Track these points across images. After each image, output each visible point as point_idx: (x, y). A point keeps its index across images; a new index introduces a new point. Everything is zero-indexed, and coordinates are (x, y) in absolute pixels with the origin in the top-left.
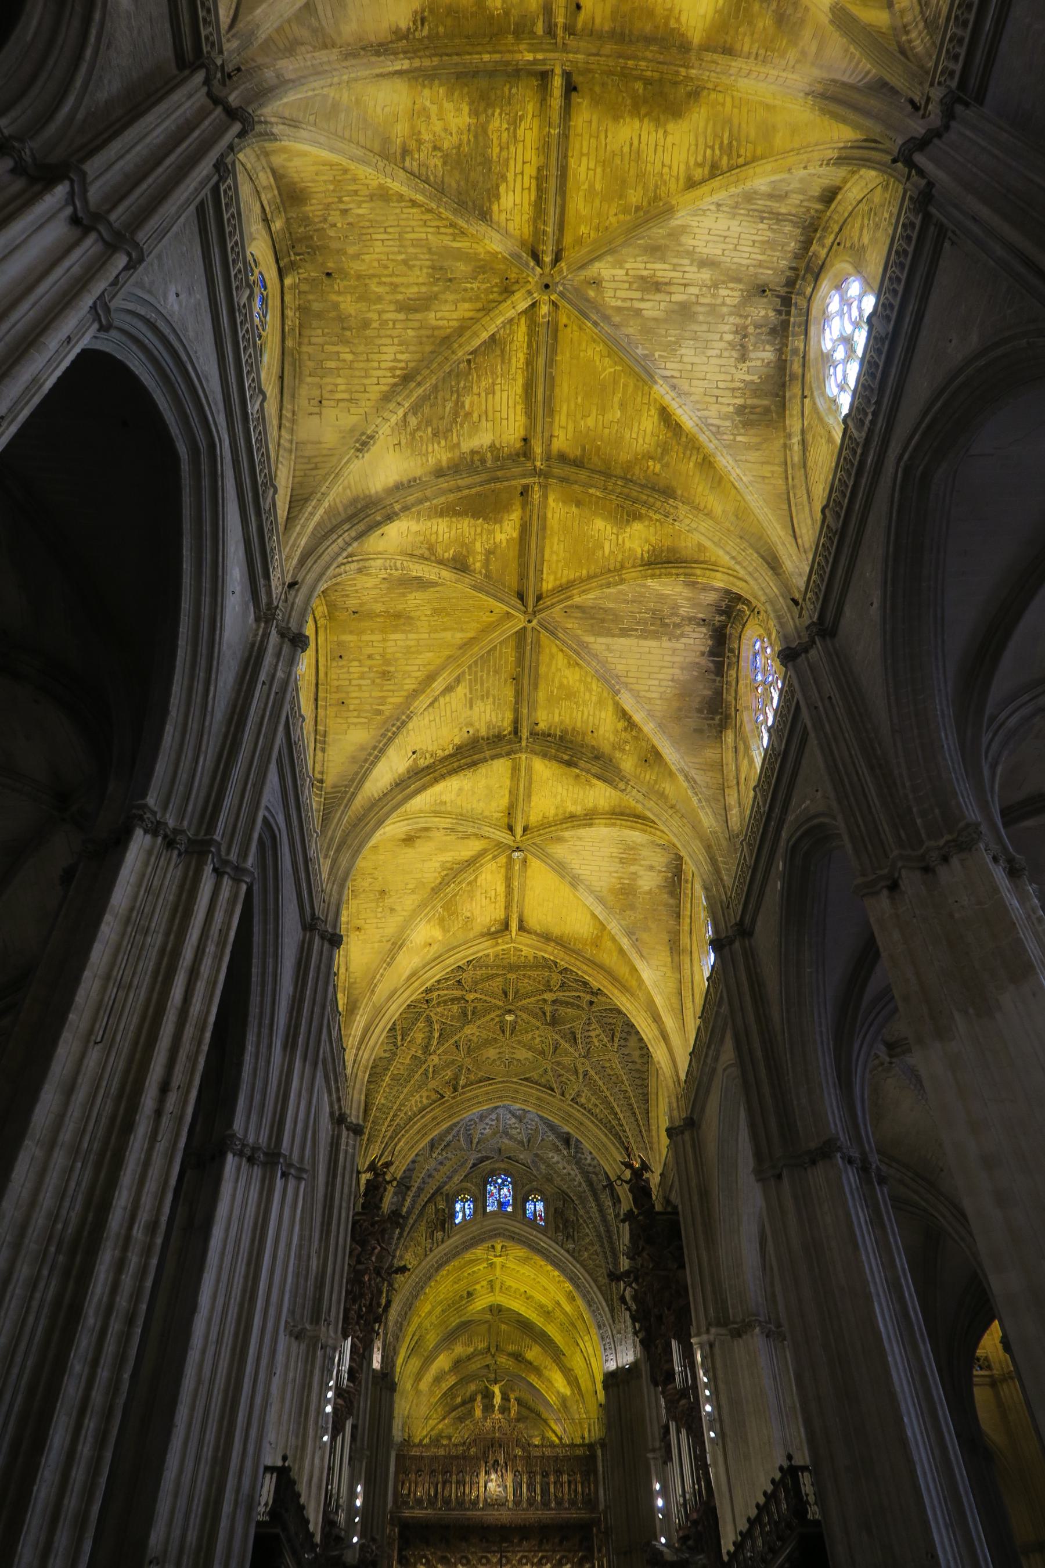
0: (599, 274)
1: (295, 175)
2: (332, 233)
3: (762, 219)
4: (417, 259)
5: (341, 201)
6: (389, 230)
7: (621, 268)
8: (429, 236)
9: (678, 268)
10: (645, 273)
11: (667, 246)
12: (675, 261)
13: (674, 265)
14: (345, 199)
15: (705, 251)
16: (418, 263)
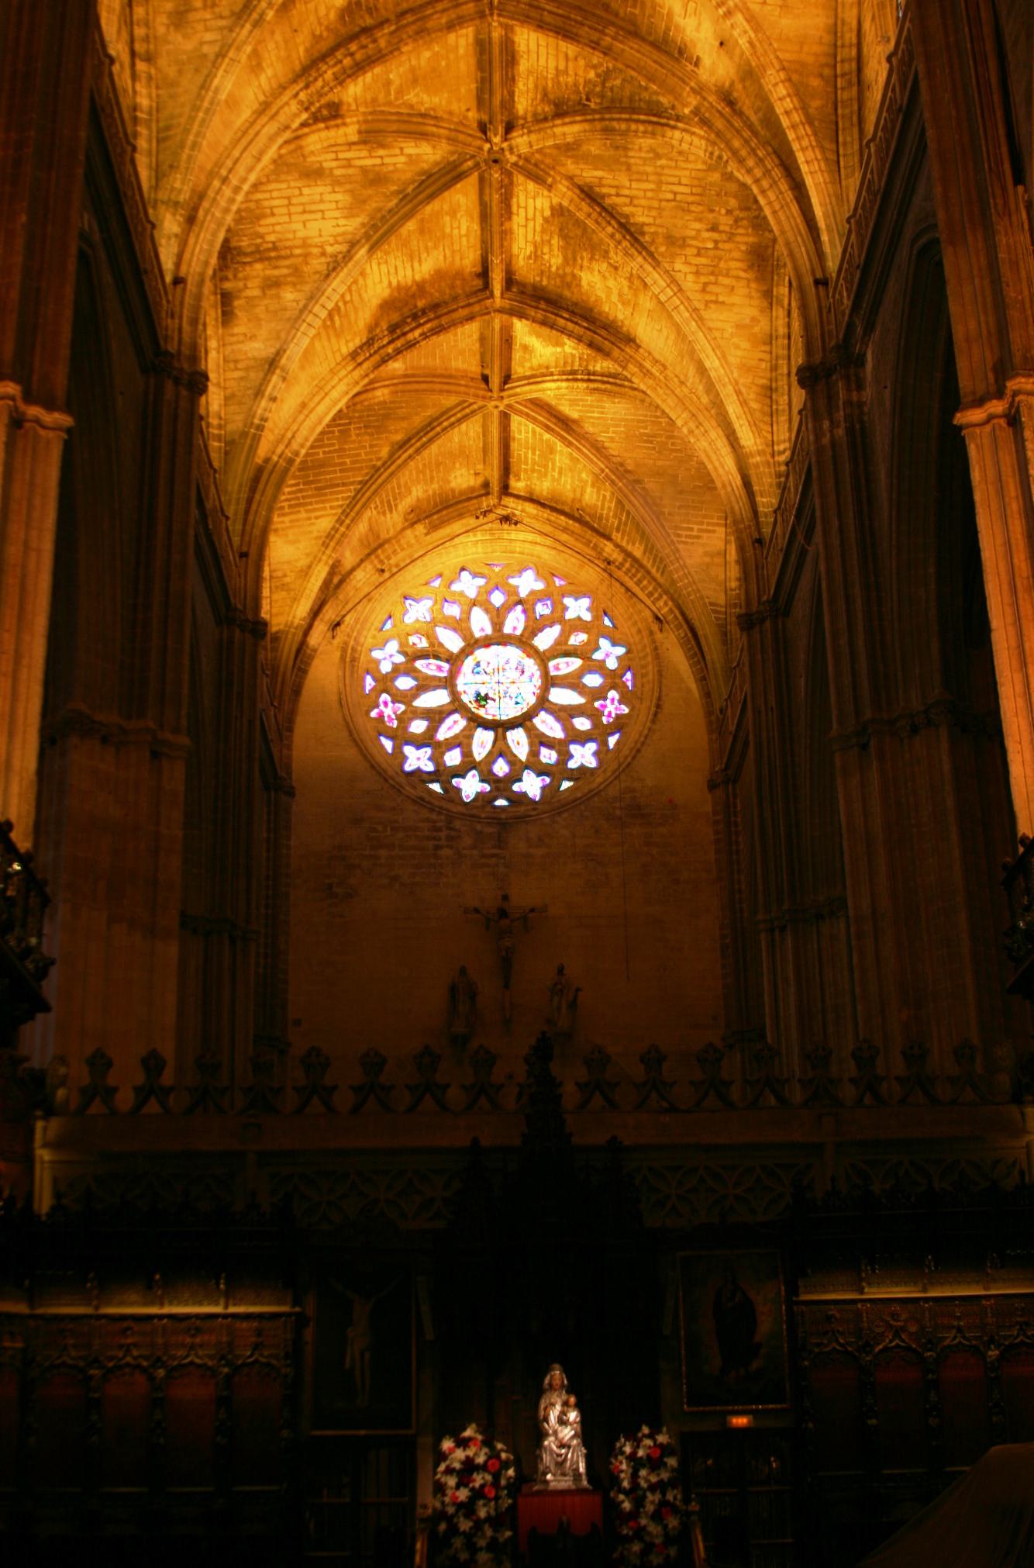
0: (434, 147)
1: (754, 294)
2: (733, 203)
3: (275, 248)
4: (645, 159)
5: (716, 242)
6: (670, 196)
7: (410, 156)
8: (627, 184)
9: (345, 163)
10: (381, 152)
11: (364, 187)
12: (351, 171)
13: (350, 166)
14: (710, 245)
15: (320, 189)
16: (643, 155)
